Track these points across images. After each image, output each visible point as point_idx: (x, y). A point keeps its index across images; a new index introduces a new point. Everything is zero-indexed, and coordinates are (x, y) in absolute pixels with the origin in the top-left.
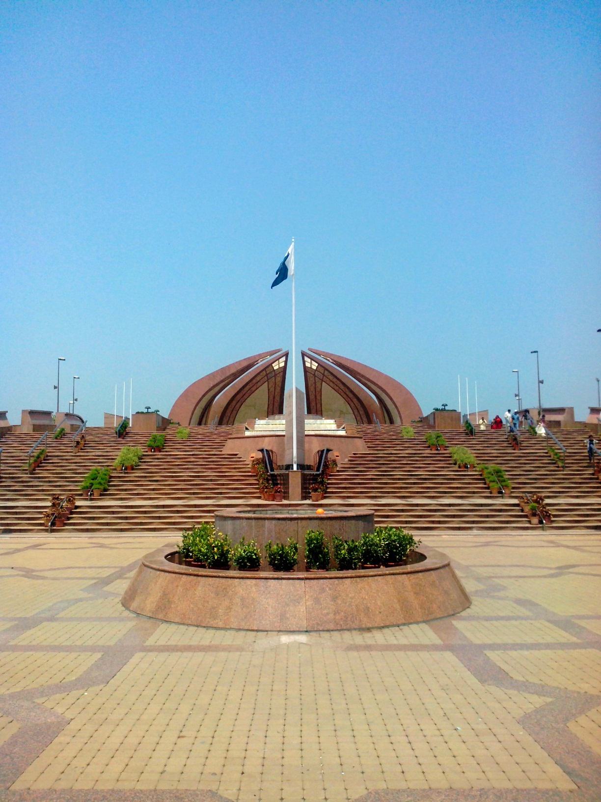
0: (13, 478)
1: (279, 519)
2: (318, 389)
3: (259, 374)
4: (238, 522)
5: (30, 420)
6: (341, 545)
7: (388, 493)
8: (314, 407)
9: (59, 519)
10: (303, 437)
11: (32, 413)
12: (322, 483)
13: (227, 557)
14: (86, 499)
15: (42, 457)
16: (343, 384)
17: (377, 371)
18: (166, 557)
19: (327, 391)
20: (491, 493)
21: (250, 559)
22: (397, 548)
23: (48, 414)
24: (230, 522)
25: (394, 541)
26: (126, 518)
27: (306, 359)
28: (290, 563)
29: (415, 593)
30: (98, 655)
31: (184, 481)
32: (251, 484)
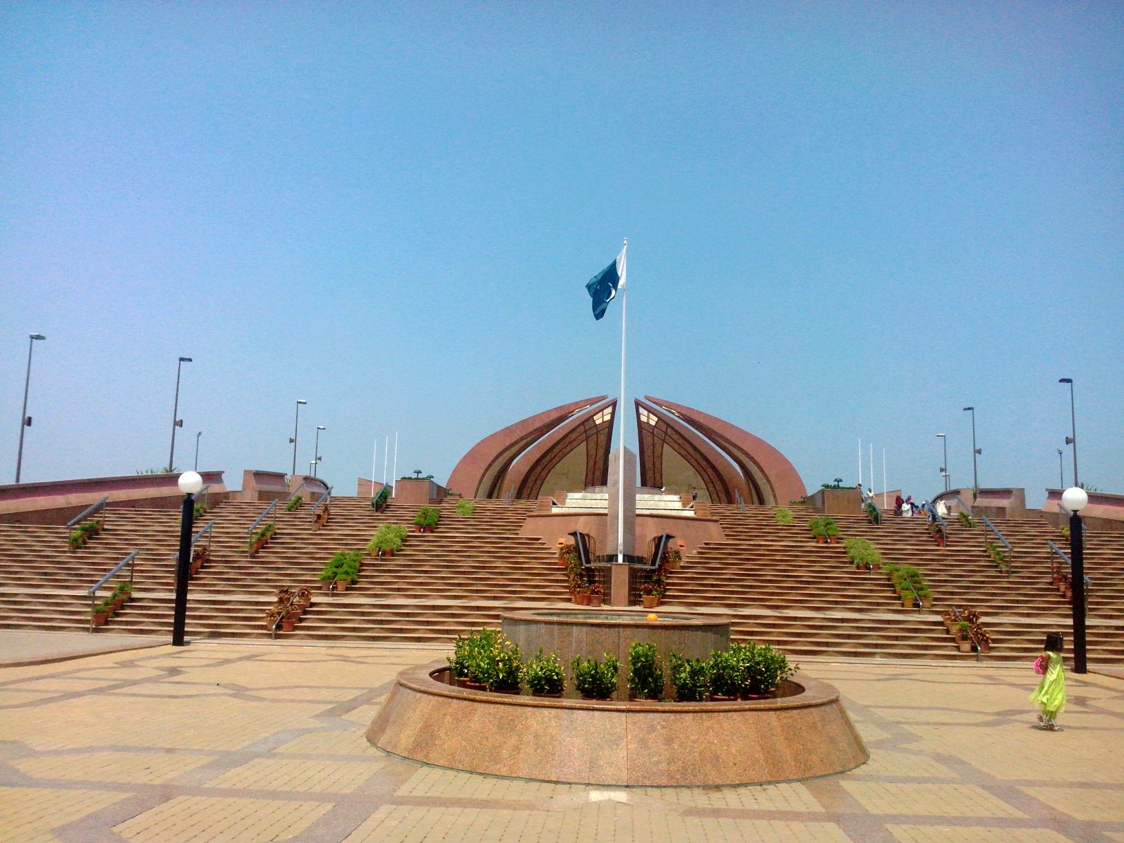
0: (226, 562)
1: (592, 625)
2: (657, 453)
3: (574, 430)
4: (534, 627)
5: (253, 483)
6: (681, 666)
7: (755, 600)
8: (652, 479)
9: (287, 622)
10: (632, 518)
11: (259, 475)
12: (659, 582)
13: (516, 678)
14: (327, 595)
15: (269, 534)
16: (695, 449)
17: (742, 431)
18: (431, 675)
19: (670, 457)
20: (903, 605)
21: (549, 680)
22: (761, 673)
23: (280, 477)
24: (522, 628)
25: (758, 663)
26: (381, 622)
27: (641, 410)
28: (607, 689)
29: (786, 739)
30: (329, 806)
31: (464, 573)
32: (557, 581)
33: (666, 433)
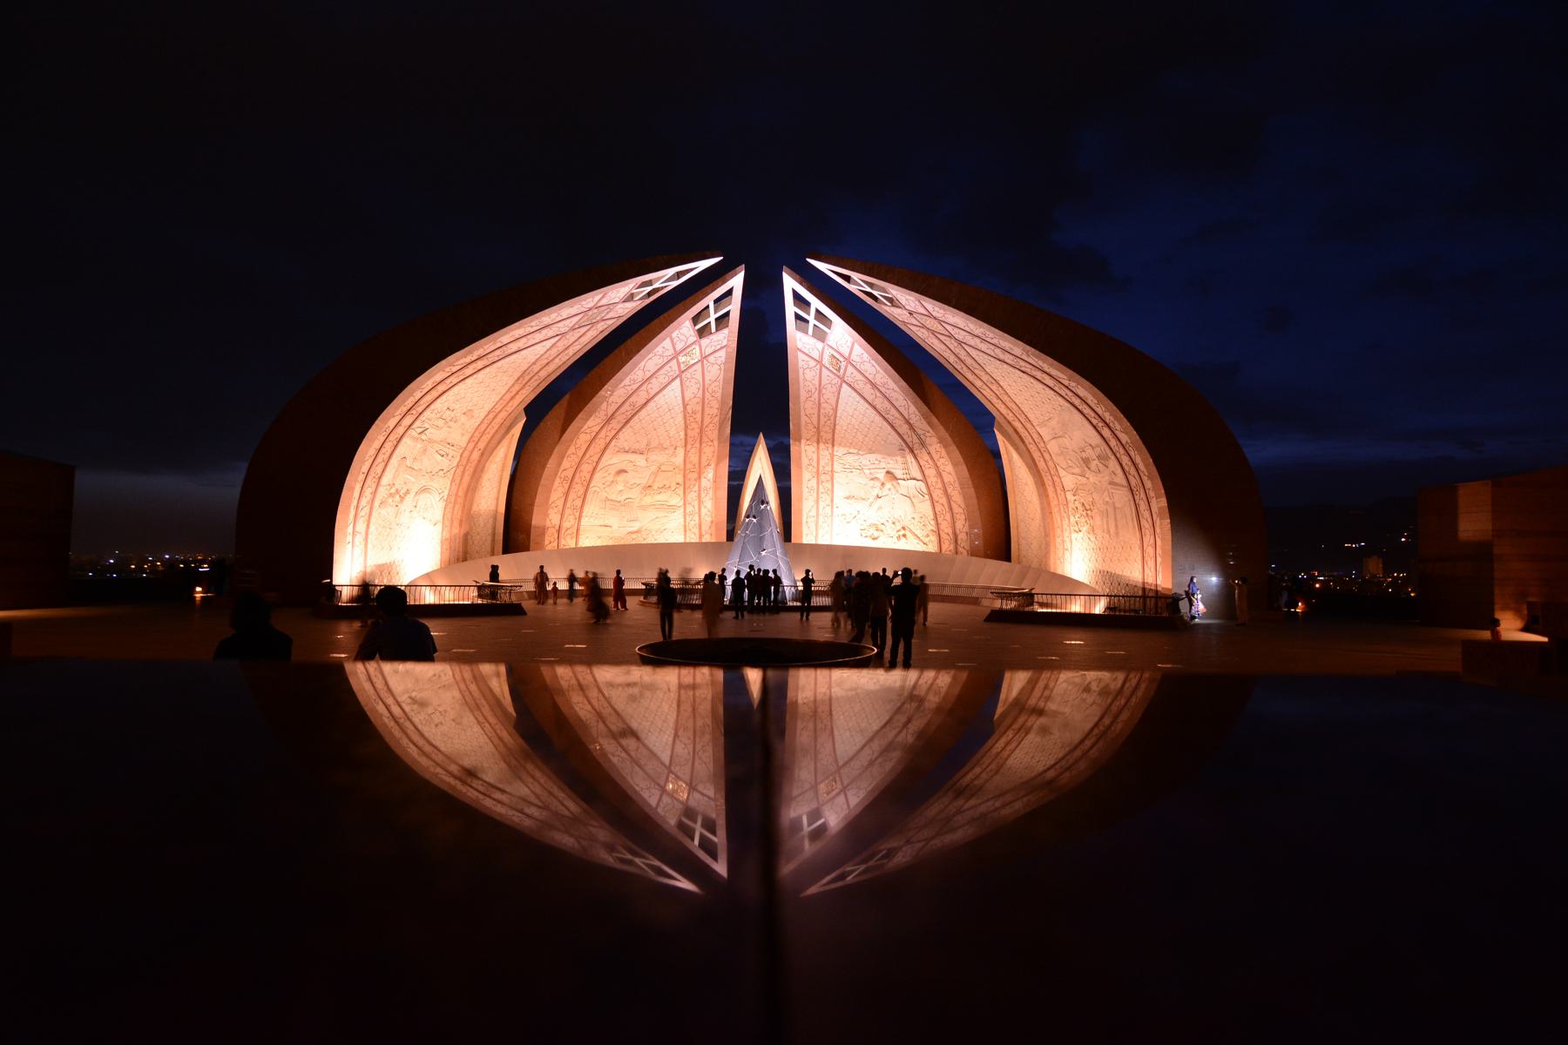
33: (848, 360)
